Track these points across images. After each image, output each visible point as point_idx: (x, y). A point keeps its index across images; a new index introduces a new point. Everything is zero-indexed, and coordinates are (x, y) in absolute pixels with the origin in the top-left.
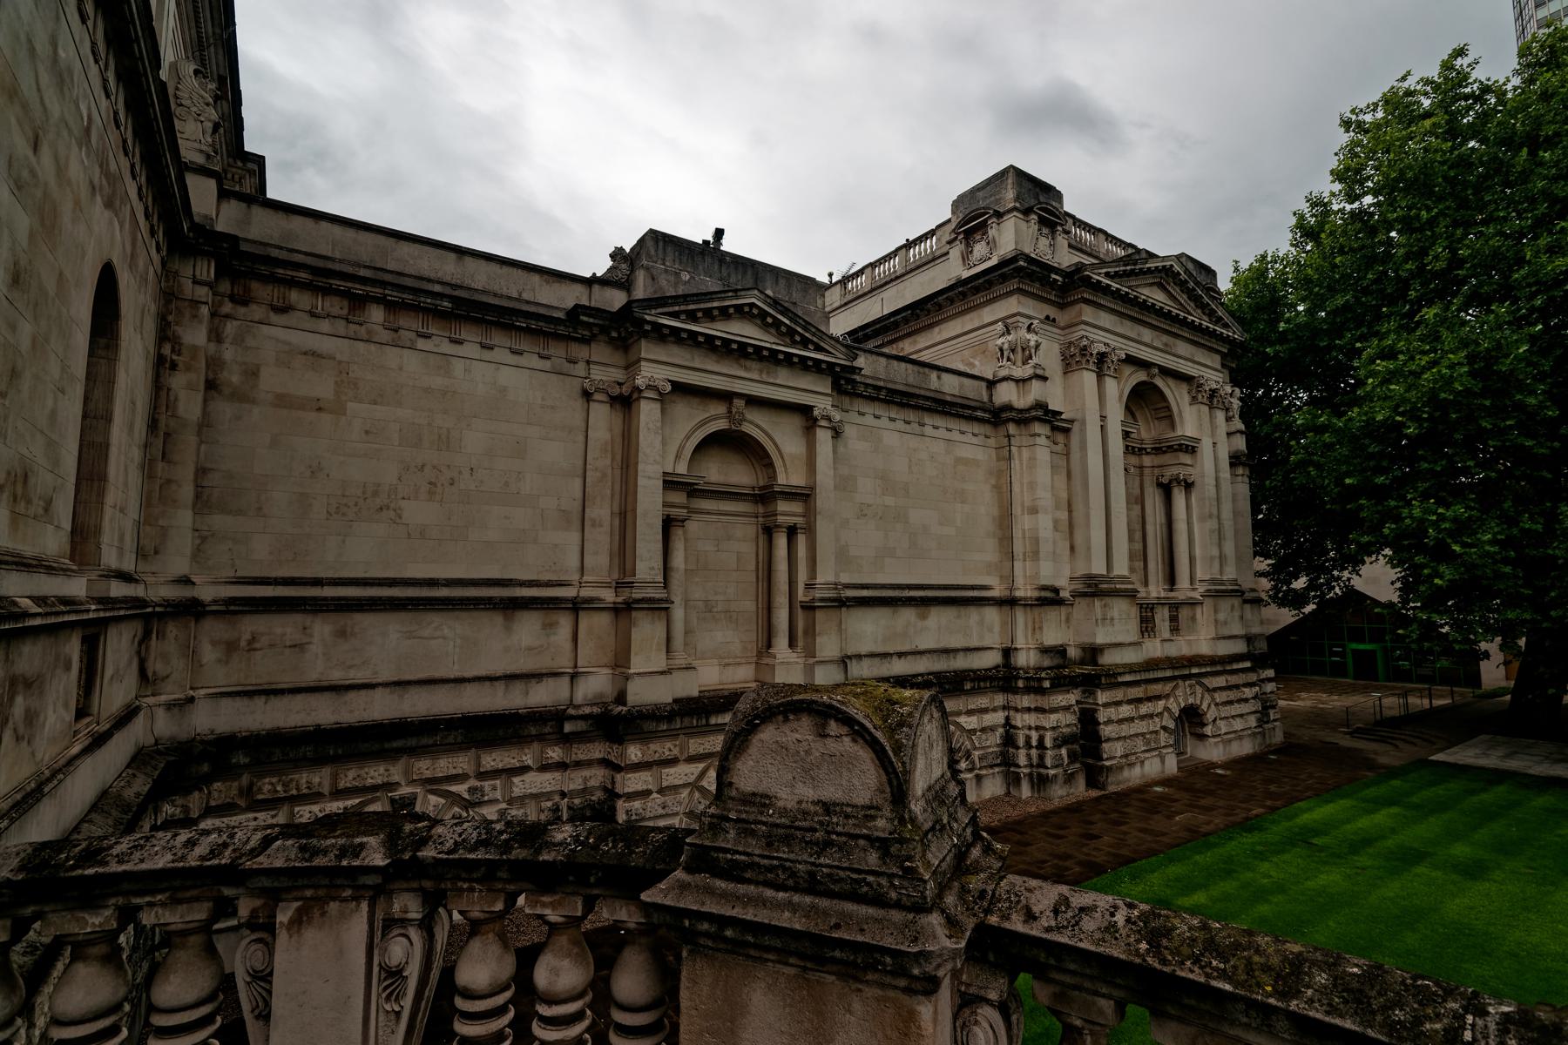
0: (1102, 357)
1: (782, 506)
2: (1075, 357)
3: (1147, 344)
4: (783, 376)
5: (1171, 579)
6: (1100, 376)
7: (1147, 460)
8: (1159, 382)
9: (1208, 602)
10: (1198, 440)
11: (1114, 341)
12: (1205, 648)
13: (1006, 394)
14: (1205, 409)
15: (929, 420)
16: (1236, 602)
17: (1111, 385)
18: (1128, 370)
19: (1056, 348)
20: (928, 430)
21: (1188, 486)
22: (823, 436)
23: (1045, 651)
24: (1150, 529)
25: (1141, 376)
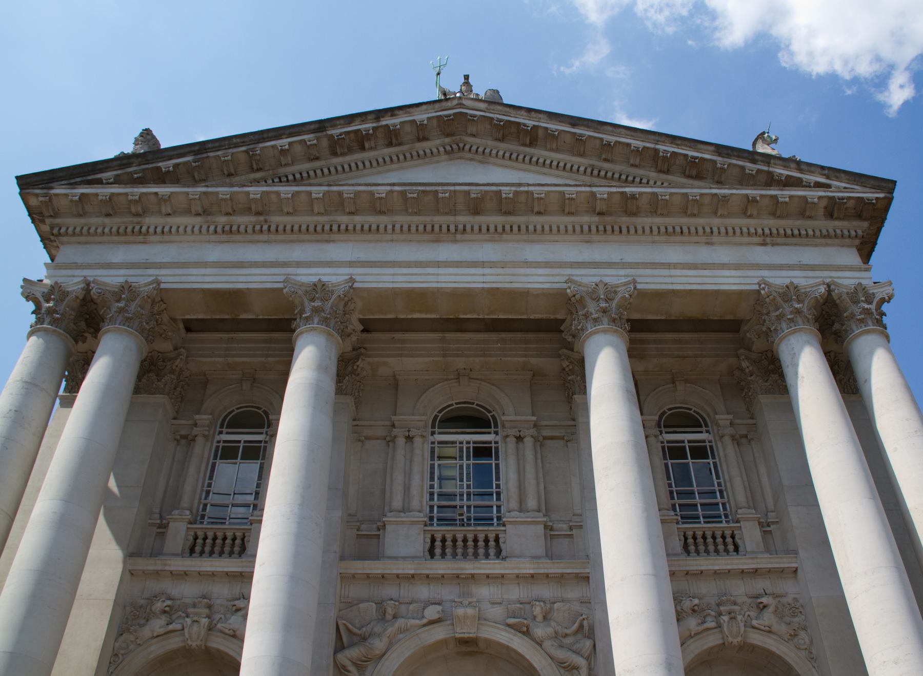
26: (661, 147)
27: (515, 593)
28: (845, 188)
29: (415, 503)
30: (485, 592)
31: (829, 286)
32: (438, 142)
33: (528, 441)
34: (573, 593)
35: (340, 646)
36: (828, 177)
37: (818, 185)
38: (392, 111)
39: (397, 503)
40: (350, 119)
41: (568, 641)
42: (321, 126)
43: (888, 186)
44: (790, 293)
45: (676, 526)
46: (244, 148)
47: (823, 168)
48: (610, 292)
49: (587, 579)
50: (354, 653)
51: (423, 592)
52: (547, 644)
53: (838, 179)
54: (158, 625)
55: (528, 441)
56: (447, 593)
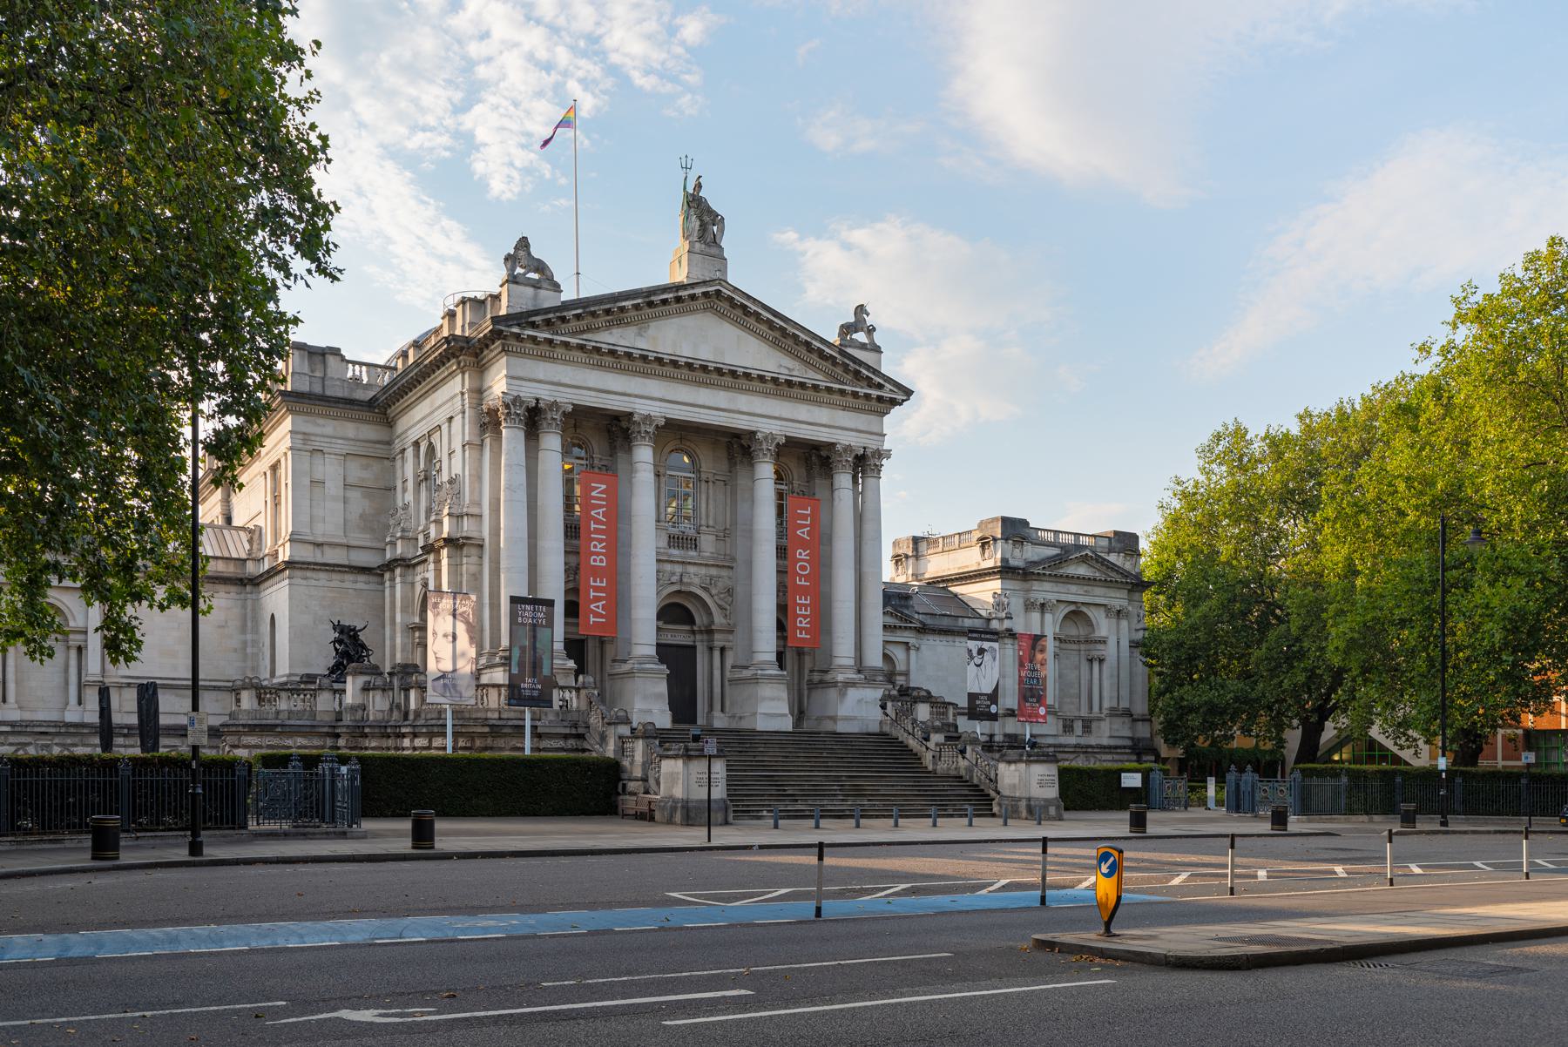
0: (1043, 605)
1: (898, 678)
2: (1029, 606)
3: (1074, 593)
4: (899, 633)
5: (1091, 708)
6: (1043, 613)
7: (1083, 647)
8: (1084, 609)
9: (1108, 719)
10: (1107, 638)
11: (1049, 596)
12: (1105, 742)
13: (995, 625)
14: (1114, 620)
15: (958, 639)
16: (1127, 720)
17: (1048, 617)
18: (1062, 606)
19: (1021, 601)
20: (957, 644)
21: (1101, 661)
22: (912, 652)
23: (1006, 735)
24: (1082, 682)
25: (1072, 608)
26: (814, 342)
27: (703, 571)
30: (692, 569)
31: (865, 448)
33: (711, 484)
34: (724, 573)
41: (722, 596)
43: (908, 393)
44: (848, 449)
49: (732, 568)
52: (716, 597)
53: (889, 383)
55: (711, 484)
56: (678, 569)
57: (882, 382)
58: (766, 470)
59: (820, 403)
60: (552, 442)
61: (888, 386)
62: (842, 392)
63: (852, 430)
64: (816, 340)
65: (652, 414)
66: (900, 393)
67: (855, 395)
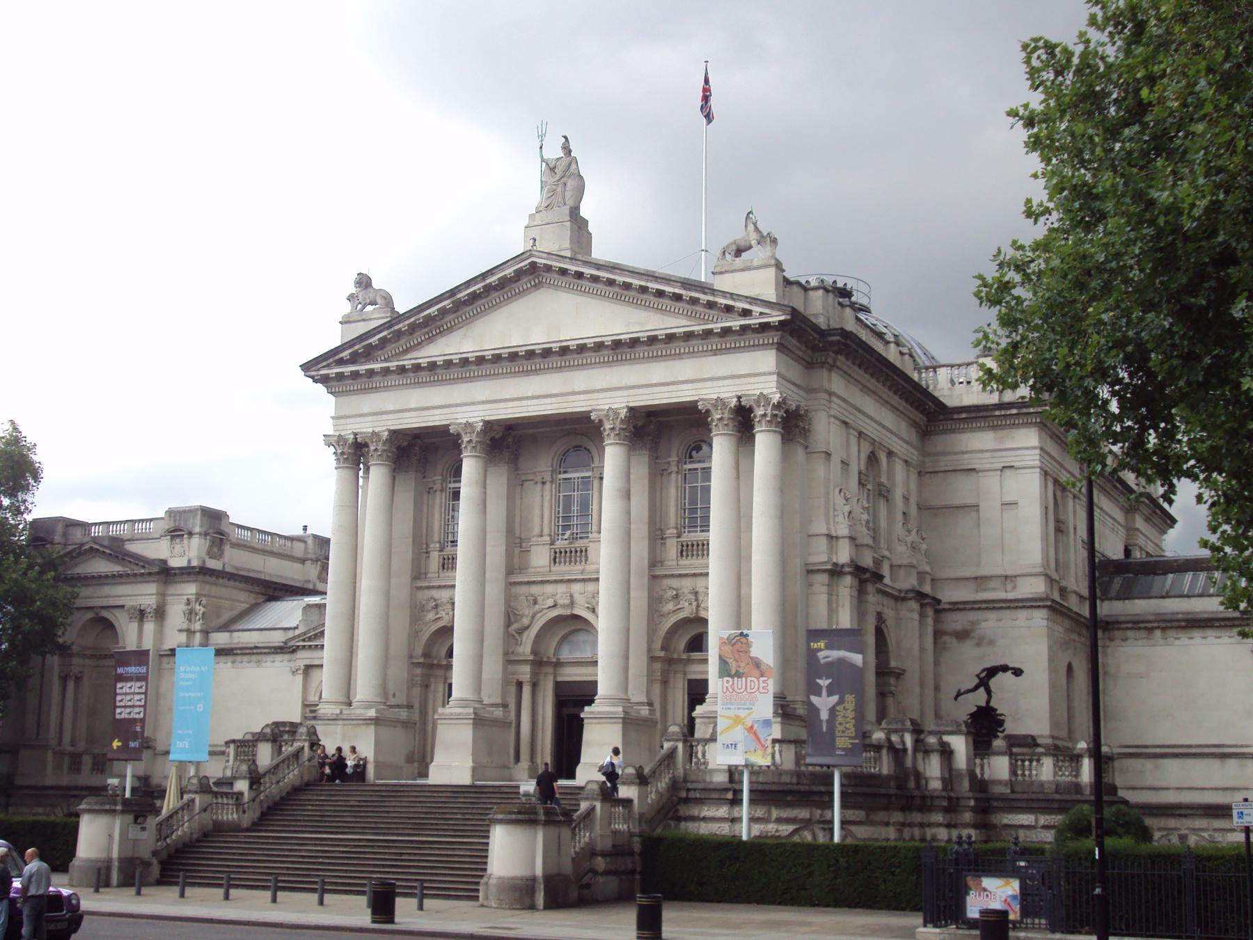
26: (650, 285)
28: (761, 313)
29: (546, 531)
32: (526, 280)
35: (508, 623)
36: (750, 303)
37: (746, 313)
38: (490, 272)
39: (537, 531)
40: (468, 284)
42: (453, 292)
45: (676, 540)
46: (412, 320)
47: (747, 297)
48: (616, 412)
50: (515, 626)
51: (549, 589)
53: (756, 305)
54: (431, 616)
57: (747, 306)
58: (612, 457)
59: (680, 356)
60: (376, 477)
61: (756, 309)
62: (708, 333)
63: (725, 378)
64: (651, 281)
65: (471, 420)
66: (774, 313)
67: (726, 332)
